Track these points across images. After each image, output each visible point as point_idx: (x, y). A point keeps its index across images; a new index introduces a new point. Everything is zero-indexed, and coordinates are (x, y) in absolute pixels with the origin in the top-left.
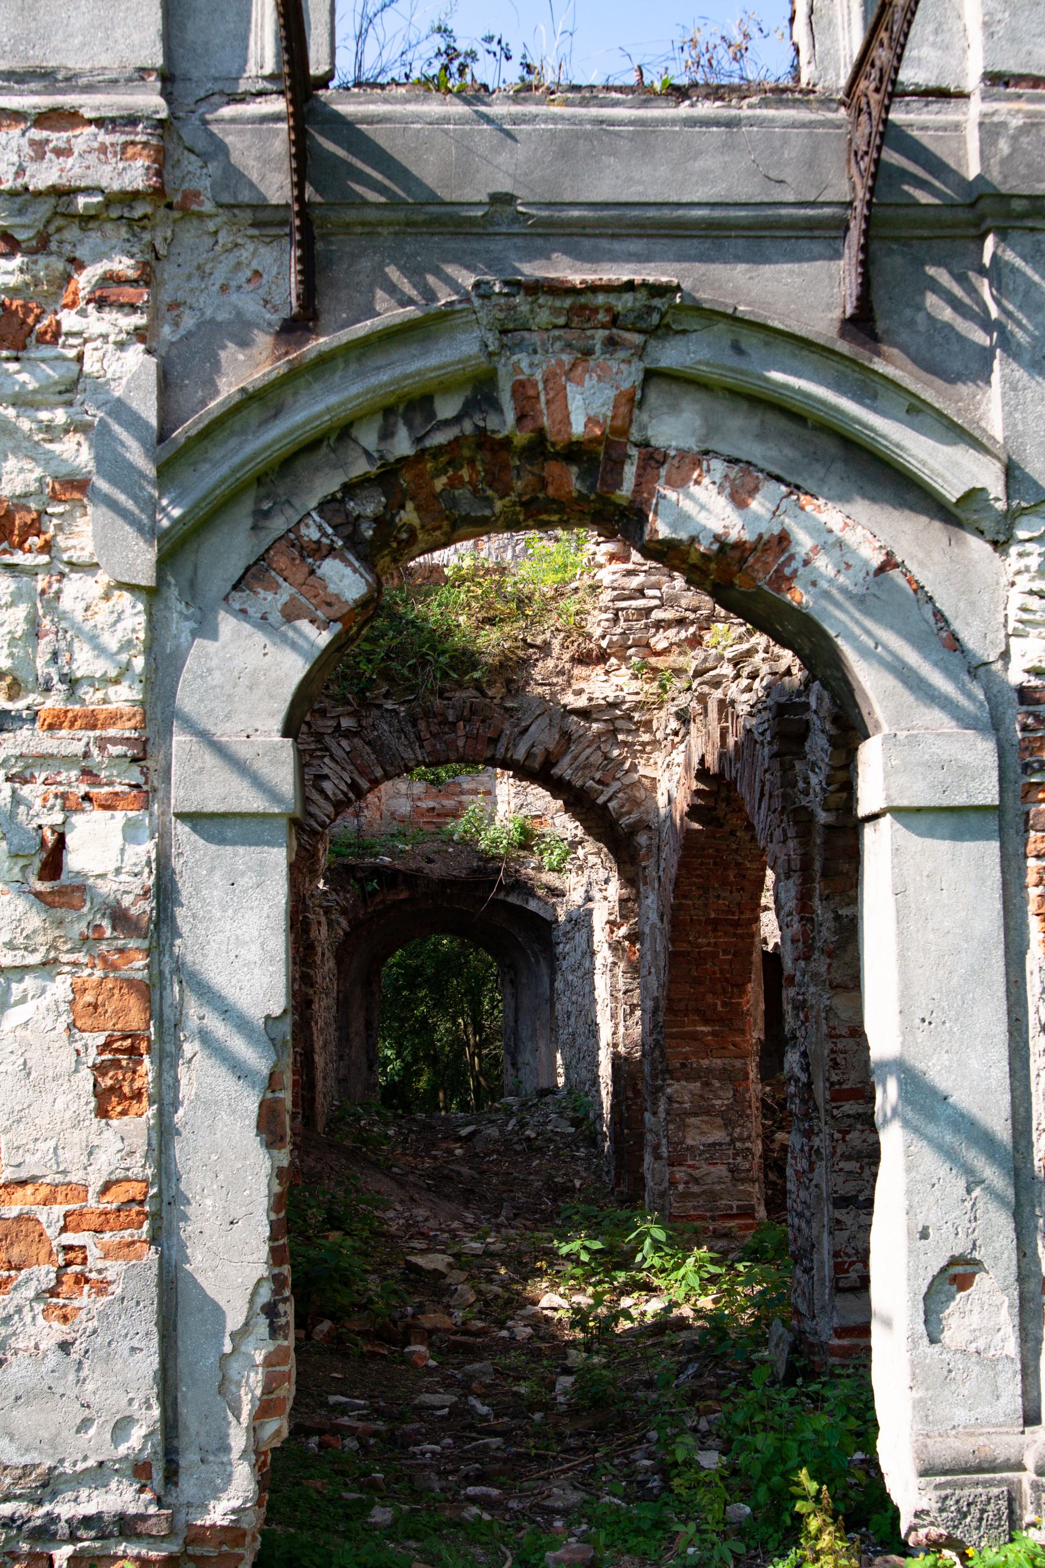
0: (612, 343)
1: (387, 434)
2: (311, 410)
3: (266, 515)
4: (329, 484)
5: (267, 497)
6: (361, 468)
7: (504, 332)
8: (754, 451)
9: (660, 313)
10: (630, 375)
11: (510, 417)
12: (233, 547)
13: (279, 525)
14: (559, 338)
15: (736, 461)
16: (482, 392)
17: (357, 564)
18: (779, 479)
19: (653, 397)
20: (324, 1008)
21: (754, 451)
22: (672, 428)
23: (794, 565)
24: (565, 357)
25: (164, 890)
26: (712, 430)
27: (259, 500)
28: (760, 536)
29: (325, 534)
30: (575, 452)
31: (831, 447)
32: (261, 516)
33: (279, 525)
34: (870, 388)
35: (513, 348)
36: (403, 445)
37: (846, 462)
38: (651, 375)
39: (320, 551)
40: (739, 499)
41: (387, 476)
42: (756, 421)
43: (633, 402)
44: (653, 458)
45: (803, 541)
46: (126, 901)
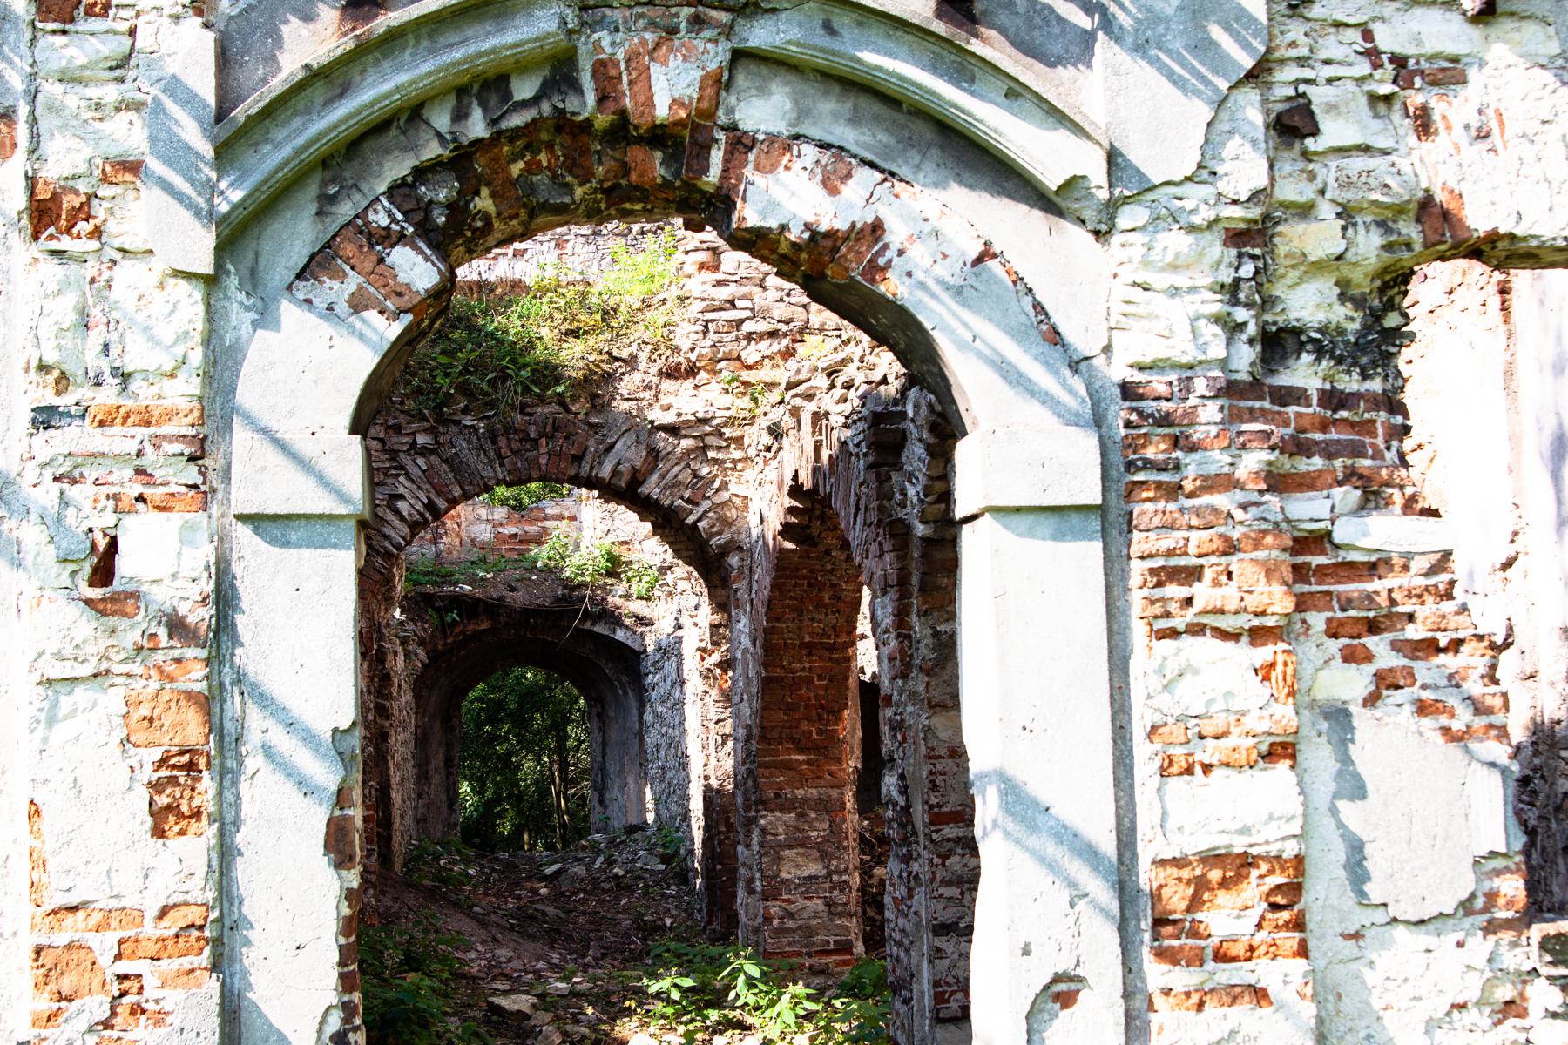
0: (697, 22)
1: (460, 116)
2: (379, 88)
3: (333, 199)
4: (398, 168)
5: (333, 181)
6: (432, 150)
7: (584, 8)
8: (846, 135)
10: (716, 56)
11: (591, 98)
12: (297, 235)
13: (345, 210)
14: (642, 16)
15: (828, 146)
16: (560, 70)
17: (429, 252)
18: (872, 165)
19: (741, 80)
20: (401, 743)
21: (846, 135)
22: (762, 110)
23: (888, 254)
24: (648, 36)
25: (224, 598)
26: (802, 114)
27: (324, 184)
28: (853, 225)
29: (394, 220)
30: (659, 136)
31: (928, 134)
32: (326, 203)
33: (345, 210)
34: (966, 68)
35: (594, 26)
36: (477, 127)
37: (942, 148)
38: (740, 56)
39: (389, 238)
40: (830, 186)
41: (461, 160)
42: (849, 105)
43: (720, 84)
44: (741, 143)
45: (896, 234)
46: (182, 611)
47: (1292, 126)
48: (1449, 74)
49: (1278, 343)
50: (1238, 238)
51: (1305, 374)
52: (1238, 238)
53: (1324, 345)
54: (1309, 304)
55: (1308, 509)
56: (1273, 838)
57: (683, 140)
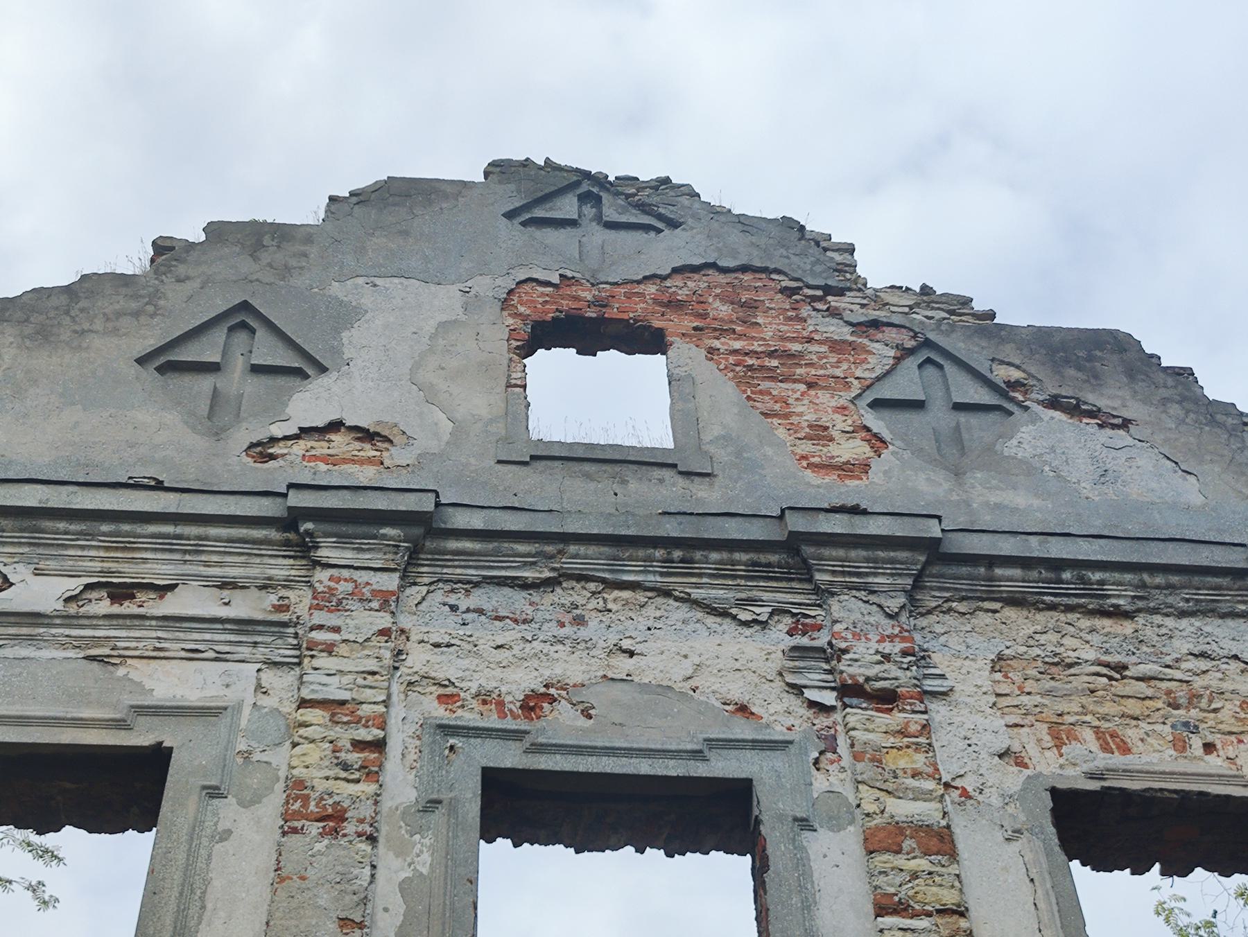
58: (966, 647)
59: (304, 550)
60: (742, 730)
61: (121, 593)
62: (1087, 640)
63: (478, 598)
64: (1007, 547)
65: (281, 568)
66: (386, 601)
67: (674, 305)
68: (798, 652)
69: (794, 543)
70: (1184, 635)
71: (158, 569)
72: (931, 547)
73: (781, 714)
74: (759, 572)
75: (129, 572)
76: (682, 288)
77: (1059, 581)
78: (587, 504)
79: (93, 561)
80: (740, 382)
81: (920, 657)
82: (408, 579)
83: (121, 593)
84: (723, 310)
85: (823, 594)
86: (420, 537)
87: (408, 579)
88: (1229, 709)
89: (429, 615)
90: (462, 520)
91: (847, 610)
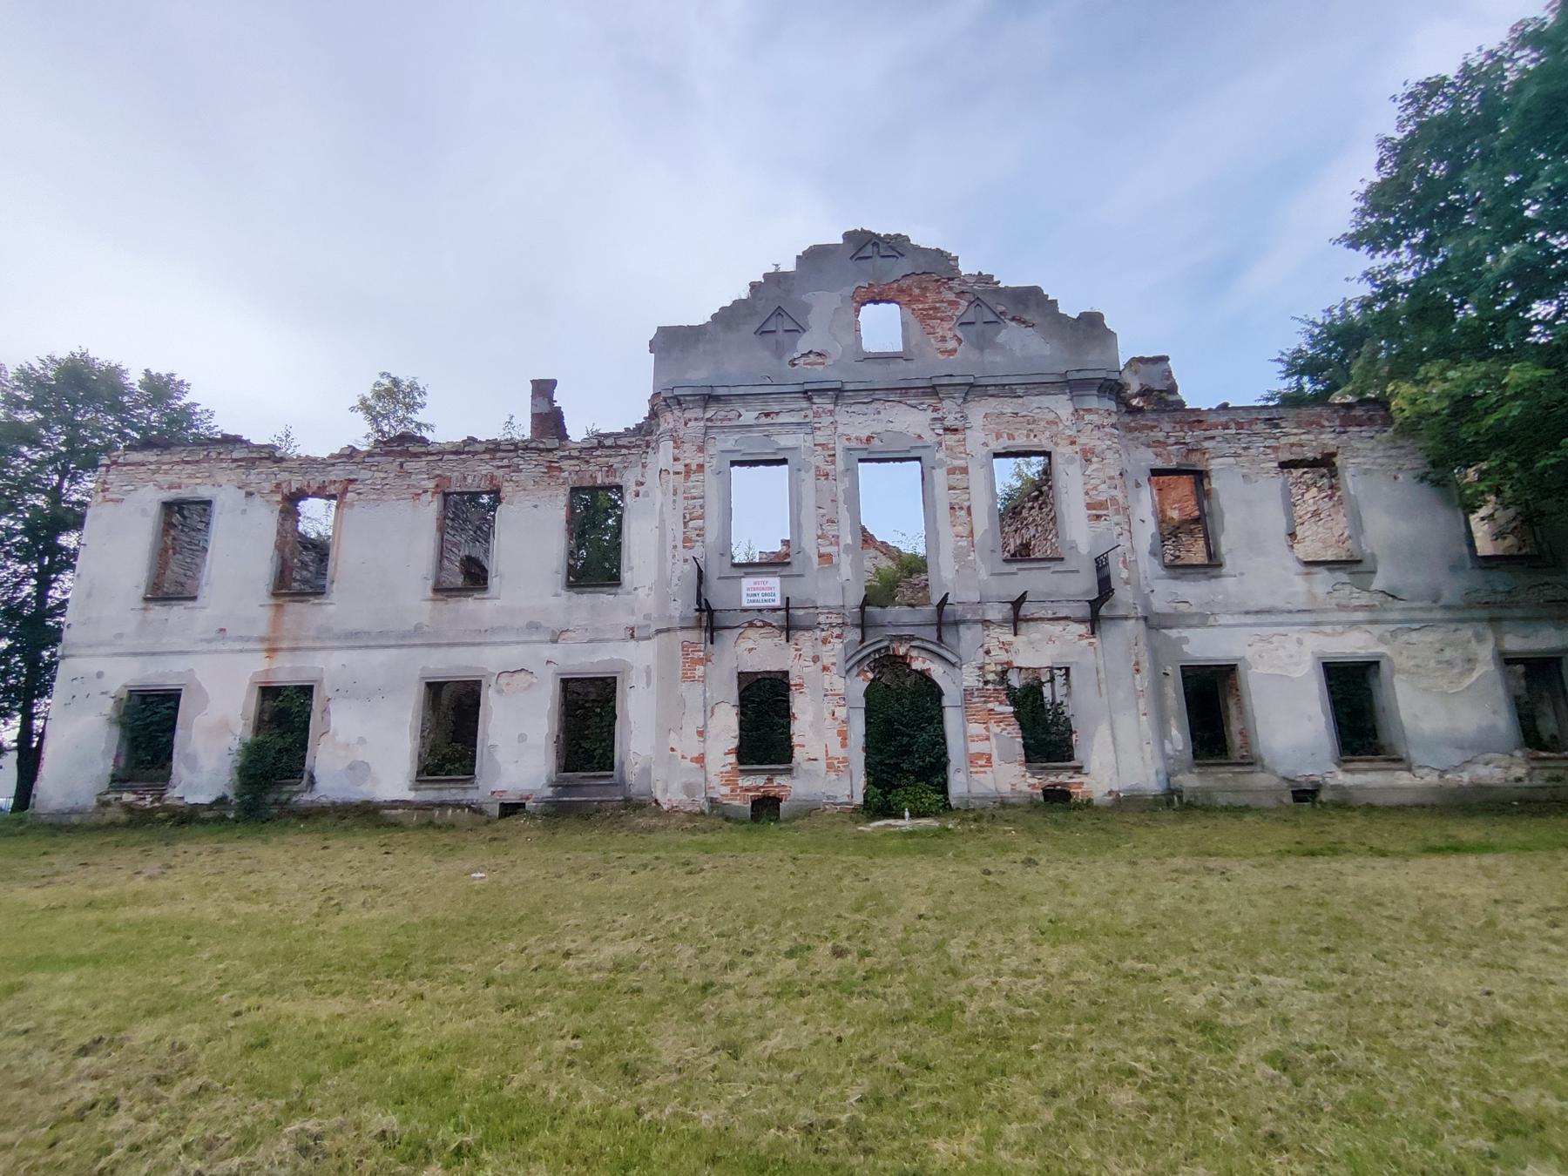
2: (865, 653)
9: (912, 638)
12: (855, 671)
16: (887, 648)
47: (988, 652)
48: (1011, 644)
49: (986, 683)
50: (980, 668)
51: (990, 686)
52: (980, 668)
53: (994, 682)
54: (991, 677)
55: (990, 706)
56: (987, 751)
57: (904, 657)
58: (978, 412)
59: (809, 399)
60: (920, 444)
61: (767, 415)
62: (1008, 406)
63: (853, 408)
64: (991, 381)
65: (804, 404)
66: (831, 413)
67: (901, 291)
68: (934, 419)
69: (934, 387)
70: (1034, 402)
71: (776, 408)
72: (971, 385)
73: (929, 438)
74: (925, 394)
75: (768, 409)
76: (905, 284)
77: (1006, 390)
78: (878, 376)
79: (759, 406)
80: (922, 321)
81: (965, 418)
82: (836, 404)
83: (767, 415)
84: (917, 291)
85: (941, 400)
86: (838, 394)
87: (836, 404)
88: (1043, 423)
89: (842, 414)
90: (848, 387)
91: (947, 403)
